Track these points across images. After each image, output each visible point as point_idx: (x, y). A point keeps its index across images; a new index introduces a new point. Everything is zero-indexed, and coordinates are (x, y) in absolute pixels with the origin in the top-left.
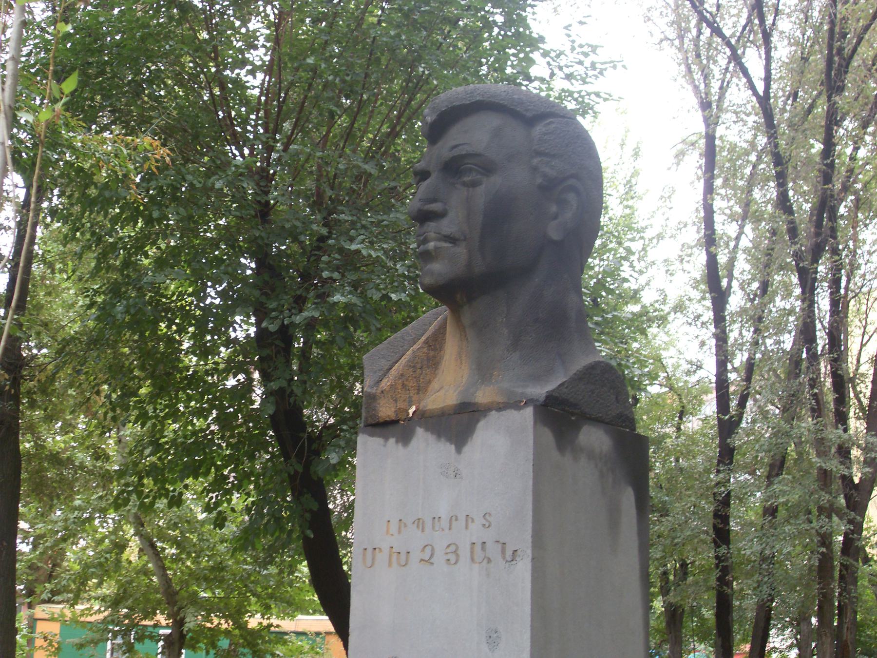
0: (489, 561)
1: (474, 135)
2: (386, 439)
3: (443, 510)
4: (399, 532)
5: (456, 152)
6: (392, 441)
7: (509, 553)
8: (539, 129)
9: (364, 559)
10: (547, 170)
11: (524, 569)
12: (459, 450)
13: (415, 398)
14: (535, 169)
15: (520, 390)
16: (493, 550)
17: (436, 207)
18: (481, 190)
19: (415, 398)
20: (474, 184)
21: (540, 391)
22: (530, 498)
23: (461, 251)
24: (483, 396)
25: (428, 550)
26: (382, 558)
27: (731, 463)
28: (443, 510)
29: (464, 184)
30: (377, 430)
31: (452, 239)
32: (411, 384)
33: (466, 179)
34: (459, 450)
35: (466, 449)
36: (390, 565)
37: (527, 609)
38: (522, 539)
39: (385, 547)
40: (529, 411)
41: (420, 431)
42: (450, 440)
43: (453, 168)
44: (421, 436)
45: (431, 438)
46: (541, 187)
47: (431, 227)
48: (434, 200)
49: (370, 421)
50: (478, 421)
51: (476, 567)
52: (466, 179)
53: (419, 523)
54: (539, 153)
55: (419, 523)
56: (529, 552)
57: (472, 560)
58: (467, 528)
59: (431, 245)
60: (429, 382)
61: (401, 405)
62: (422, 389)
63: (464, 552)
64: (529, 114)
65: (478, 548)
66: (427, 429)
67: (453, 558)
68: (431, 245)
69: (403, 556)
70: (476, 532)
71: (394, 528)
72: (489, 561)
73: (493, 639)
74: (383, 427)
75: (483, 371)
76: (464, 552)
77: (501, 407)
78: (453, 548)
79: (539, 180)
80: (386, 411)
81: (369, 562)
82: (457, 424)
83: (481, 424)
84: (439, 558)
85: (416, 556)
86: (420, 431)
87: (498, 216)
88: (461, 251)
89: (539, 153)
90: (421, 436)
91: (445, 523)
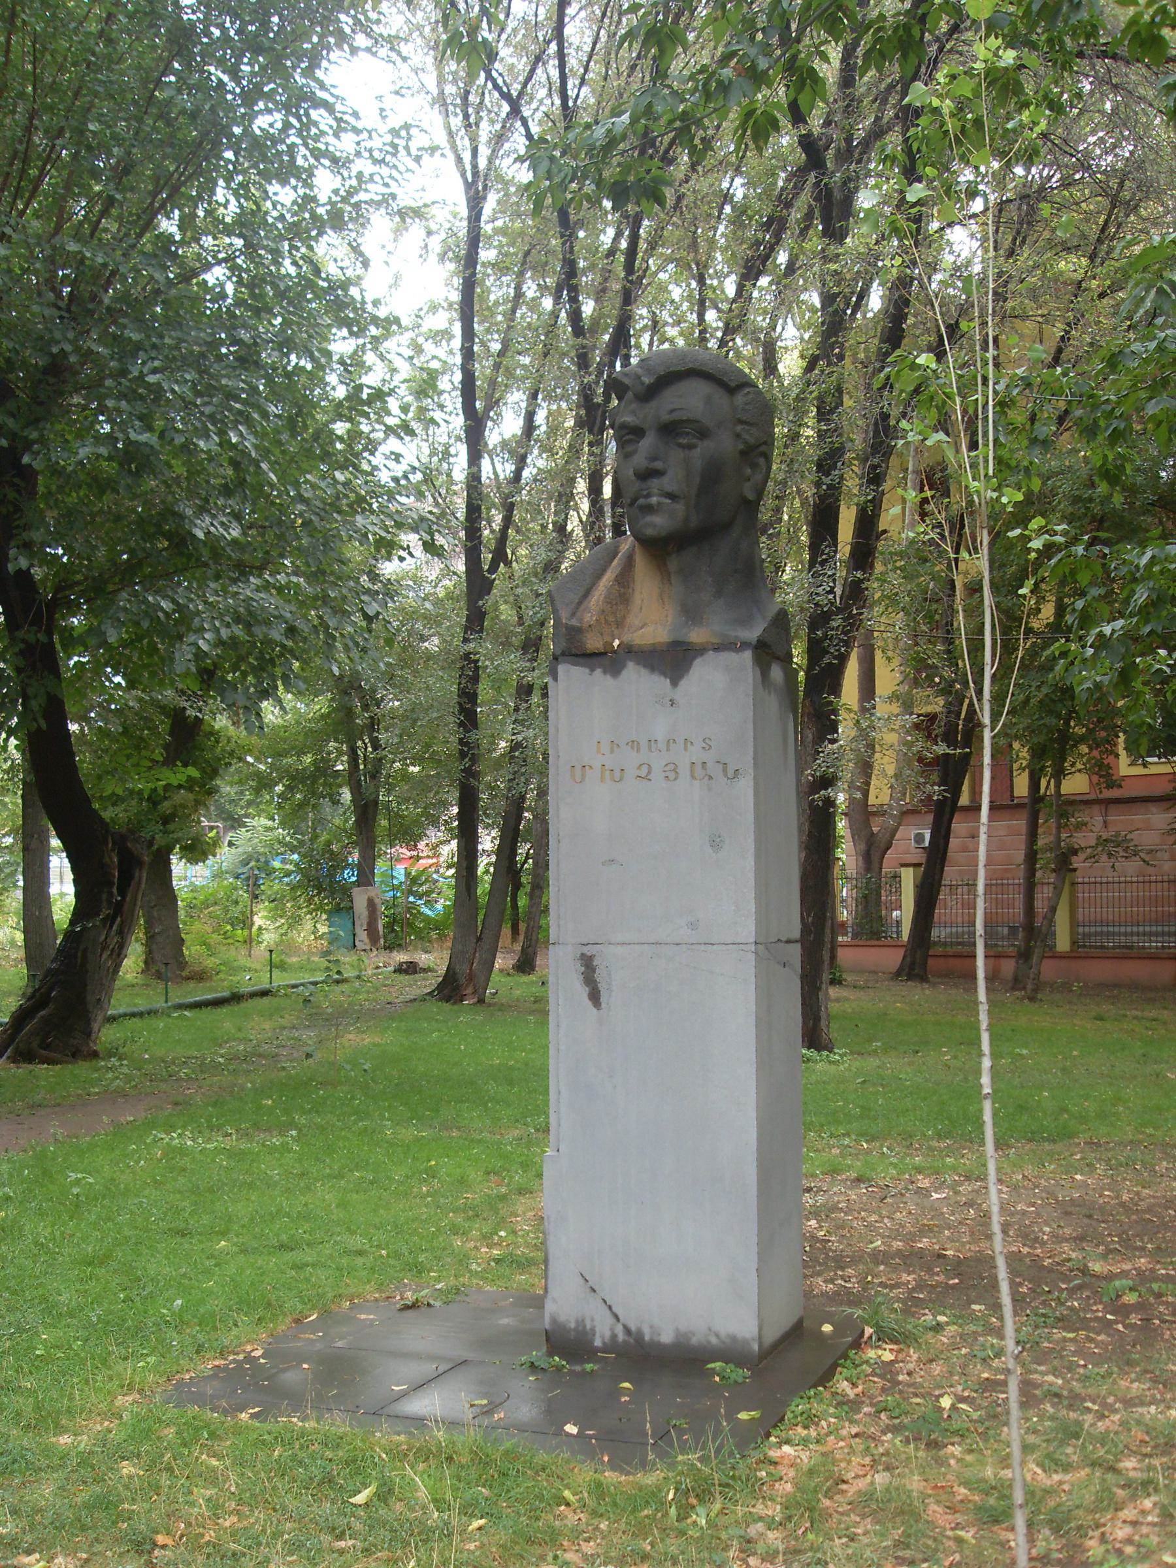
0: (710, 778)
1: (690, 400)
2: (592, 670)
3: (660, 732)
4: (612, 751)
5: (676, 416)
6: (598, 672)
7: (730, 773)
8: (740, 399)
9: (573, 776)
10: (746, 437)
11: (745, 788)
12: (675, 683)
13: (616, 632)
14: (738, 436)
15: (733, 634)
17: (658, 465)
18: (697, 452)
19: (616, 632)
20: (690, 447)
21: (753, 633)
22: (750, 727)
23: (680, 507)
24: (697, 636)
25: (645, 769)
27: (481, 631)
28: (660, 732)
29: (680, 445)
30: (580, 660)
31: (672, 496)
32: (611, 619)
33: (684, 441)
34: (675, 683)
35: (683, 683)
36: (603, 779)
37: (751, 817)
38: (745, 761)
39: (597, 765)
40: (748, 655)
41: (631, 665)
42: (665, 675)
43: (670, 430)
45: (644, 672)
46: (742, 453)
47: (654, 483)
48: (654, 459)
49: (574, 651)
50: (694, 658)
51: (697, 783)
52: (684, 441)
54: (741, 422)
55: (634, 744)
56: (751, 771)
57: (693, 777)
58: (686, 749)
59: (654, 500)
60: (624, 617)
61: (608, 638)
62: (620, 624)
63: (684, 770)
64: (733, 384)
65: (698, 767)
66: (638, 663)
67: (672, 775)
68: (654, 500)
69: (617, 775)
70: (696, 753)
71: (605, 748)
72: (710, 778)
73: (716, 843)
75: (691, 614)
77: (718, 648)
78: (672, 767)
79: (741, 447)
80: (593, 643)
81: (578, 777)
82: (673, 660)
83: (698, 662)
84: (657, 774)
86: (631, 665)
87: (712, 476)
88: (680, 507)
89: (741, 422)
91: (662, 745)
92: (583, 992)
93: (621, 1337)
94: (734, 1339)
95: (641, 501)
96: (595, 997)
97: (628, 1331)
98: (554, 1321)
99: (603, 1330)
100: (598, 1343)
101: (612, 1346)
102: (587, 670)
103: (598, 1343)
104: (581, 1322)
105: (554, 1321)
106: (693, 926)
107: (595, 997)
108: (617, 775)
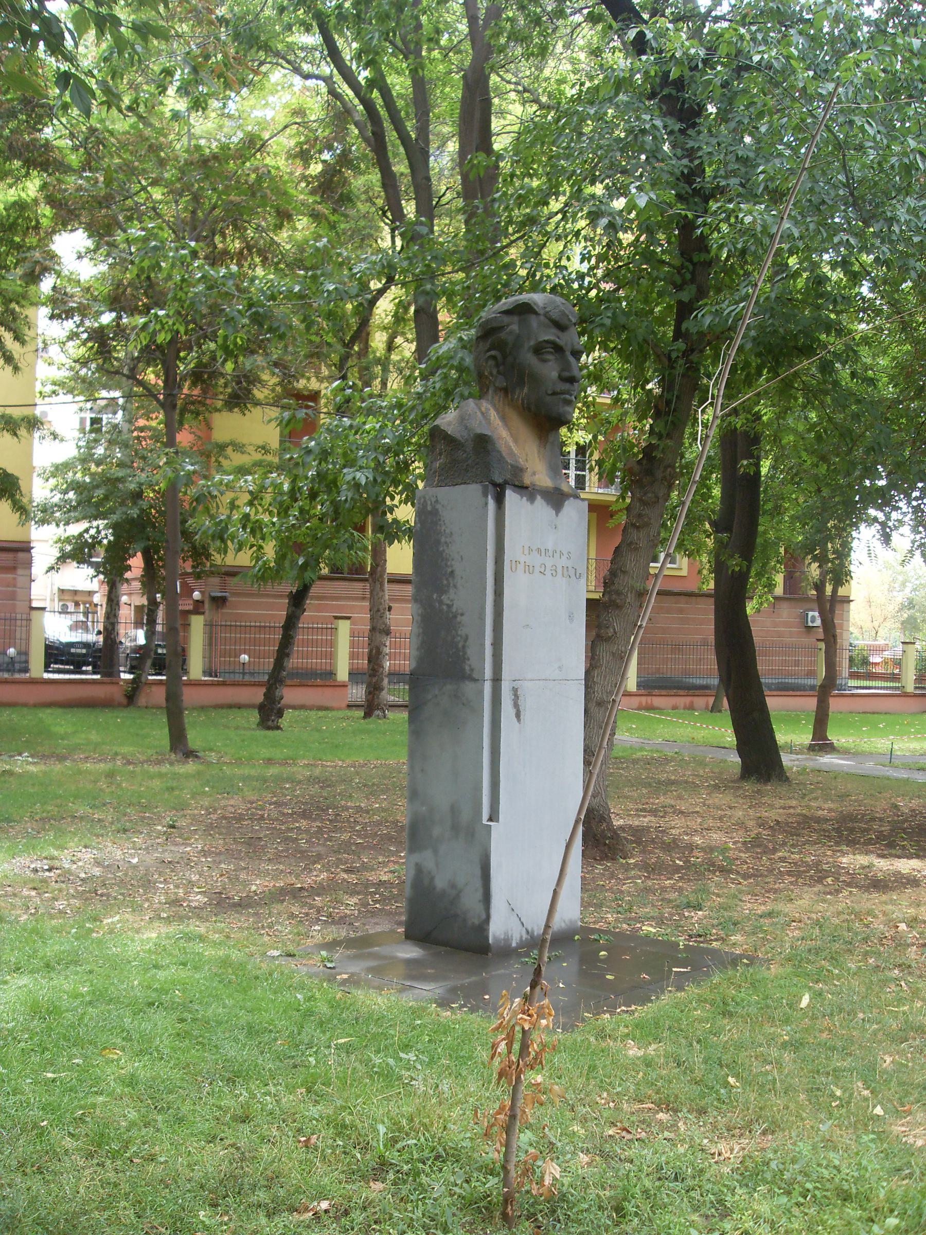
12: (557, 515)
16: (572, 572)
26: (521, 567)
34: (557, 515)
44: (539, 500)
53: (539, 550)
55: (539, 550)
63: (559, 570)
70: (564, 562)
71: (526, 552)
73: (571, 617)
74: (521, 488)
76: (559, 570)
84: (548, 572)
85: (537, 569)
86: (539, 497)
90: (539, 500)
92: (513, 712)
93: (525, 936)
94: (571, 921)
95: (568, 396)
96: (518, 715)
97: (528, 932)
98: (494, 937)
99: (517, 935)
100: (514, 945)
101: (522, 944)
102: (518, 496)
103: (514, 945)
104: (506, 933)
105: (494, 937)
106: (560, 668)
107: (518, 715)
108: (529, 569)
